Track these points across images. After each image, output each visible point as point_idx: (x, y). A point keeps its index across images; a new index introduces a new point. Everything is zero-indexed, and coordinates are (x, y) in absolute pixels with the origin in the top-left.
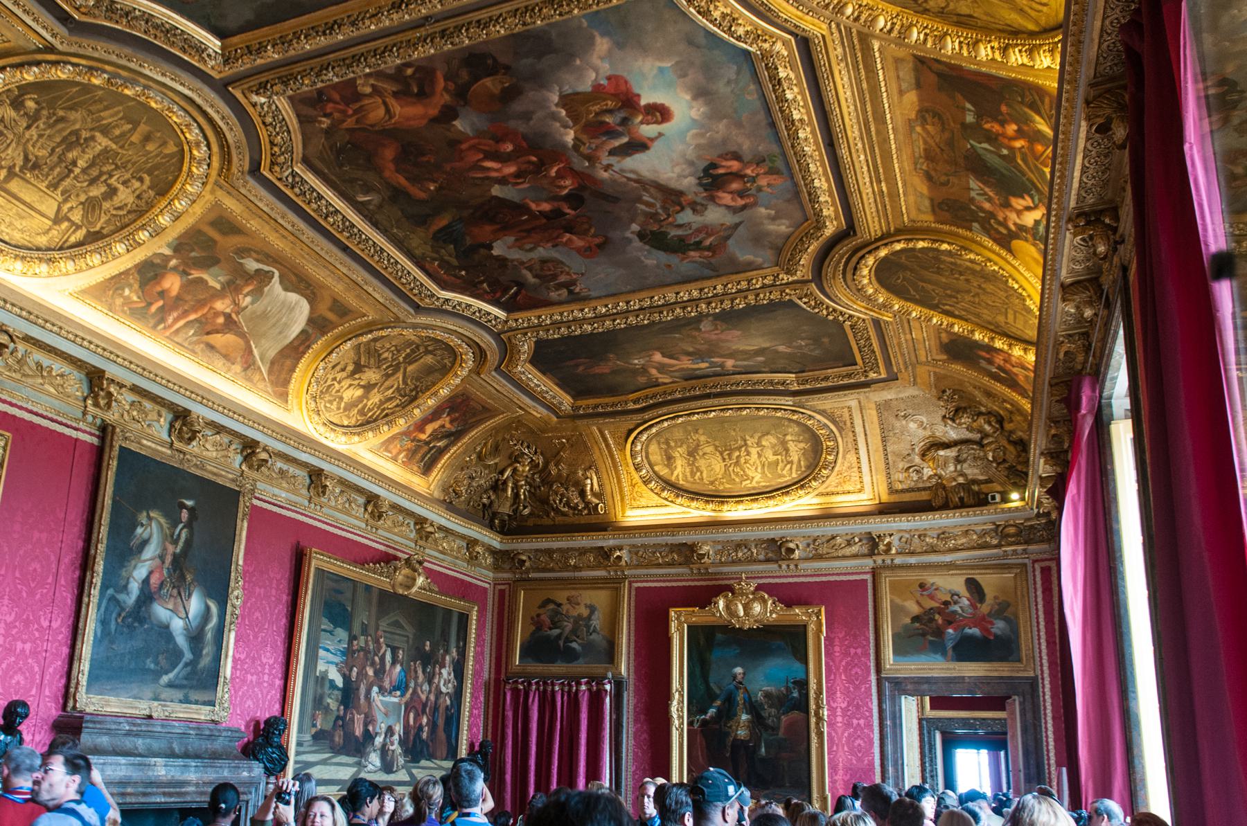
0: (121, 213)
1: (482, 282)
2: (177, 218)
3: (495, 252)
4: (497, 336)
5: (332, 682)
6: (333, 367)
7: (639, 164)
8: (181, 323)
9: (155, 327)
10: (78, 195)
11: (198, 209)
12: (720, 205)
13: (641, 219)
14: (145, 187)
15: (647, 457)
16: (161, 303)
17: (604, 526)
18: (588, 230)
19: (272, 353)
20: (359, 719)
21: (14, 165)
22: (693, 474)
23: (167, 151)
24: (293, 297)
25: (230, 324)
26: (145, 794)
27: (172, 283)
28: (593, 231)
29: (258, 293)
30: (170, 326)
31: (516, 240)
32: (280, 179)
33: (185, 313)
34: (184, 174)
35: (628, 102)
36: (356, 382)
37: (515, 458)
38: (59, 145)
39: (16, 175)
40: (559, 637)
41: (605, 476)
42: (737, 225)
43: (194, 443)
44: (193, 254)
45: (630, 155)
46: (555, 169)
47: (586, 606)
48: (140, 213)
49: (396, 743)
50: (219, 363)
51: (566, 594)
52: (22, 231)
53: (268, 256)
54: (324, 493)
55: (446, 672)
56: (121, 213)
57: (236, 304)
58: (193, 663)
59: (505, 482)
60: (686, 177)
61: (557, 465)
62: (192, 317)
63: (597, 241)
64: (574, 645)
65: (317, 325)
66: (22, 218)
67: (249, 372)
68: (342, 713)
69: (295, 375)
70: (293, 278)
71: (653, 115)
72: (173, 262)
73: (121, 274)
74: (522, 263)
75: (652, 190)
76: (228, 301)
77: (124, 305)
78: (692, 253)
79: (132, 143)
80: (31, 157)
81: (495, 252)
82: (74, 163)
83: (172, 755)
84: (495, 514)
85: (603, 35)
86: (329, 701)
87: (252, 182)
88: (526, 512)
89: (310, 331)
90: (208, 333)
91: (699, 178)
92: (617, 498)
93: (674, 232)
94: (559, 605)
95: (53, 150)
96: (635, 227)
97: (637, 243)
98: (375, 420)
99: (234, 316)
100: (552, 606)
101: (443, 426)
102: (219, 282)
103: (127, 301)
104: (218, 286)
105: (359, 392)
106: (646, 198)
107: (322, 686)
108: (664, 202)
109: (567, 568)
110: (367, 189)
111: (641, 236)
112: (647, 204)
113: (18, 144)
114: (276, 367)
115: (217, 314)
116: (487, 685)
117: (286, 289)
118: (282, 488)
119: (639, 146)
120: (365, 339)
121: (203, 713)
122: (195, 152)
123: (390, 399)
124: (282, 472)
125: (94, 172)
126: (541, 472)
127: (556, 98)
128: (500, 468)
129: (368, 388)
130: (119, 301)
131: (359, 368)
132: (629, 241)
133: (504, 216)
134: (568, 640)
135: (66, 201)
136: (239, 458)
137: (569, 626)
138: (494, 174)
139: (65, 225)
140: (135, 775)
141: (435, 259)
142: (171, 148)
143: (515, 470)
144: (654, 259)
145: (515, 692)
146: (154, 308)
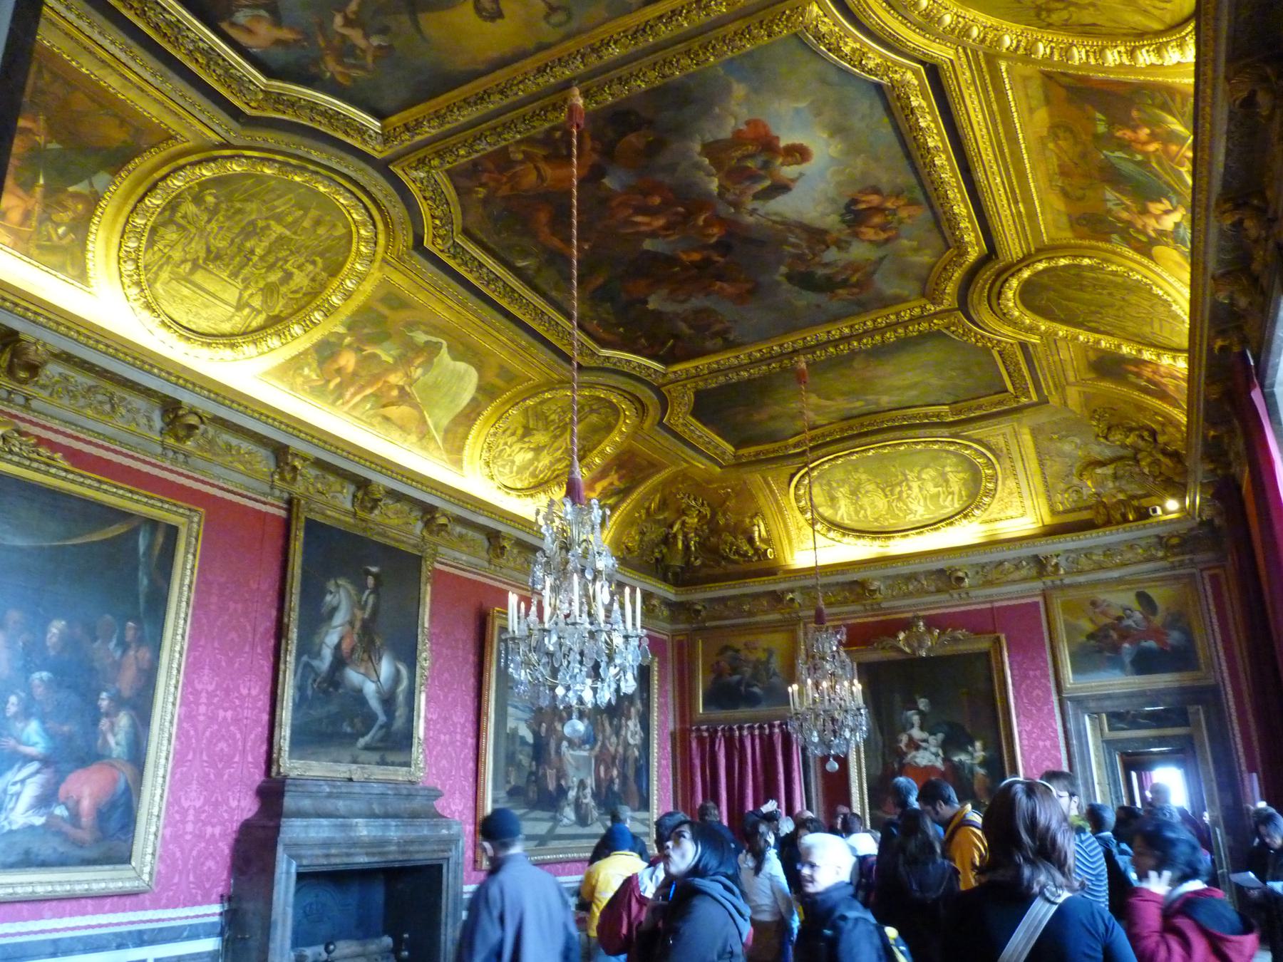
0: (297, 296)
1: (639, 337)
2: (348, 295)
3: (651, 306)
4: (657, 390)
5: (522, 738)
6: (504, 432)
7: (783, 206)
8: (358, 398)
10: (257, 282)
11: (368, 287)
12: (863, 241)
14: (318, 270)
15: (811, 500)
16: (338, 380)
17: (772, 570)
19: (445, 422)
20: (551, 773)
21: (198, 258)
22: (857, 513)
23: (337, 233)
24: (462, 366)
25: (404, 396)
26: (348, 855)
27: (348, 360)
29: (428, 364)
30: (348, 402)
32: (442, 251)
33: (362, 388)
34: (353, 254)
35: (768, 145)
36: (526, 446)
37: (683, 512)
38: (238, 235)
39: (200, 267)
40: (739, 683)
41: (771, 522)
42: (882, 259)
43: (376, 512)
44: (366, 331)
45: (773, 198)
46: (703, 217)
47: (764, 650)
48: (314, 294)
49: (589, 796)
50: (396, 434)
51: (743, 640)
52: (208, 319)
53: (435, 327)
54: (502, 554)
55: (633, 725)
56: (297, 296)
57: (407, 375)
58: (388, 726)
59: (675, 536)
61: (724, 514)
62: (369, 391)
63: (748, 286)
64: (756, 690)
65: (486, 392)
66: (207, 307)
67: (424, 441)
68: (534, 768)
69: (468, 442)
70: (461, 347)
71: (792, 156)
72: (348, 340)
73: (300, 354)
74: (677, 315)
75: (797, 231)
76: (400, 374)
78: (840, 291)
79: (305, 228)
80: (212, 248)
81: (651, 306)
82: (252, 252)
83: (373, 815)
84: (667, 568)
85: (739, 81)
86: (521, 757)
87: (417, 257)
88: (698, 562)
89: (480, 398)
90: (384, 406)
91: (842, 215)
92: (785, 542)
93: (821, 272)
94: (737, 651)
95: (232, 241)
96: (783, 269)
97: (786, 286)
98: (546, 482)
99: (407, 388)
100: (730, 653)
101: (612, 484)
102: (391, 356)
103: (307, 380)
104: (390, 360)
105: (530, 455)
107: (514, 743)
109: (741, 614)
110: (525, 254)
111: (790, 278)
112: (794, 245)
113: (200, 237)
114: (450, 436)
115: (391, 387)
116: (673, 735)
117: (455, 359)
118: (462, 552)
119: (781, 188)
120: (530, 402)
121: (400, 774)
122: (362, 232)
123: (559, 460)
124: (461, 536)
125: (271, 259)
126: (708, 523)
127: (697, 147)
128: (669, 521)
129: (538, 450)
130: (299, 380)
131: (527, 432)
132: (779, 284)
133: (656, 269)
134: (749, 685)
135: (246, 288)
136: (420, 525)
137: (748, 671)
138: (643, 228)
139: (247, 311)
140: (338, 835)
141: (592, 319)
142: (340, 231)
143: (684, 523)
144: (805, 300)
145: (701, 740)
146: (332, 385)
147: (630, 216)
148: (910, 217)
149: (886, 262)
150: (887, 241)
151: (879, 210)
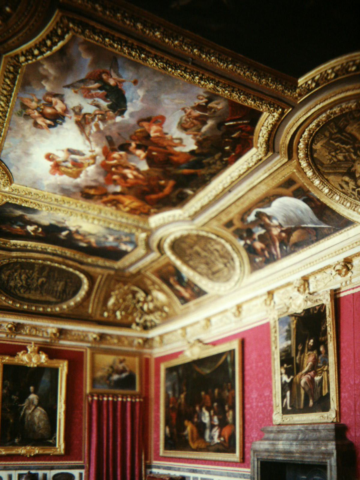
3: (195, 147)
12: (66, 105)
13: (110, 122)
18: (141, 132)
28: (139, 130)
31: (175, 146)
42: (68, 87)
60: (67, 129)
63: (145, 124)
75: (87, 132)
78: (112, 82)
81: (195, 147)
93: (104, 104)
96: (118, 119)
97: (130, 109)
106: (94, 129)
108: (89, 123)
111: (122, 113)
112: (97, 126)
117: (269, 206)
119: (71, 151)
127: (78, 180)
138: (135, 173)
147: (131, 179)
148: (32, 100)
149: (69, 82)
150: (55, 96)
151: (43, 115)
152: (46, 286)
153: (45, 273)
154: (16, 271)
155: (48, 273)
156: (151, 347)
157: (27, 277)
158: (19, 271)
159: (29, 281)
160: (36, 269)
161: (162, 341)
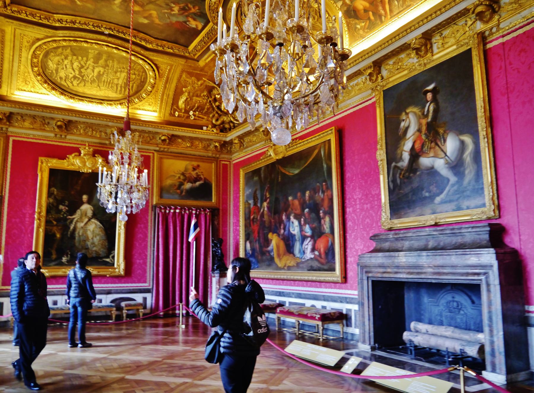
9: (382, 22)
16: (371, 13)
77: (364, 31)
103: (363, 28)
130: (361, 32)
146: (372, 18)
152: (104, 78)
153: (101, 62)
154: (66, 58)
155: (106, 61)
156: (230, 153)
157: (80, 66)
158: (70, 58)
159: (82, 70)
160: (91, 56)
161: (241, 144)
